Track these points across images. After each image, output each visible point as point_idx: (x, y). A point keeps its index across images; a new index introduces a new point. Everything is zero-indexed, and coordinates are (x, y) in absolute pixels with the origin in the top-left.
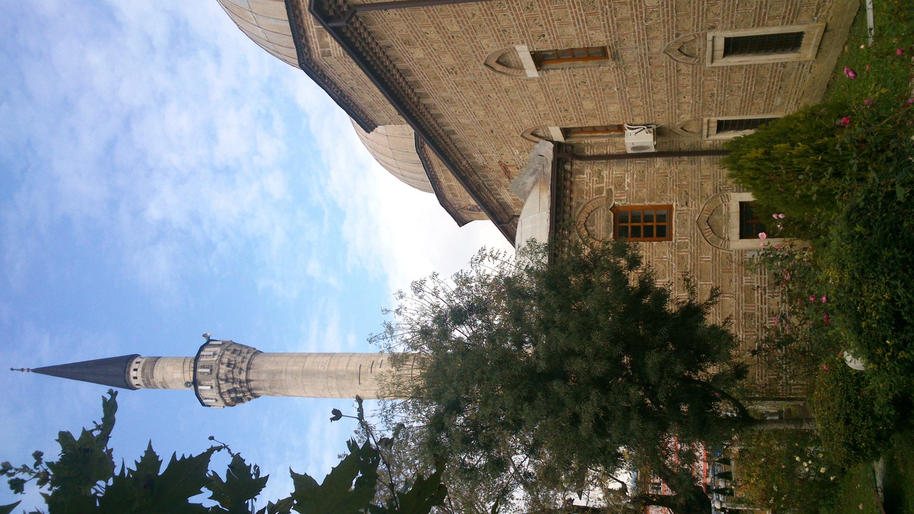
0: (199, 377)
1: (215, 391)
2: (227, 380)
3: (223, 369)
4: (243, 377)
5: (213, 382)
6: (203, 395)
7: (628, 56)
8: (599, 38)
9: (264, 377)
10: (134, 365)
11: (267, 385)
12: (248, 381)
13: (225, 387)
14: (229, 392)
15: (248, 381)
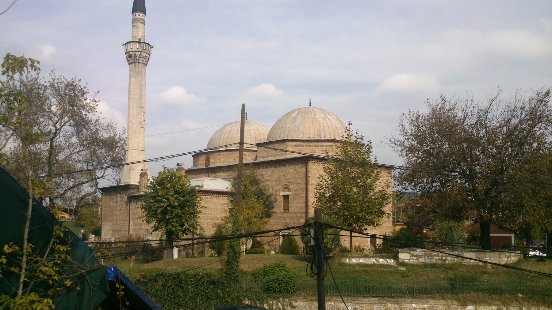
0: (142, 44)
1: (136, 50)
2: (140, 55)
3: (144, 54)
4: (141, 61)
5: (140, 50)
6: (135, 44)
7: (285, 215)
8: (292, 209)
9: (140, 69)
10: (141, 14)
11: (137, 70)
12: (139, 63)
13: (137, 54)
14: (135, 55)
15: (139, 63)
